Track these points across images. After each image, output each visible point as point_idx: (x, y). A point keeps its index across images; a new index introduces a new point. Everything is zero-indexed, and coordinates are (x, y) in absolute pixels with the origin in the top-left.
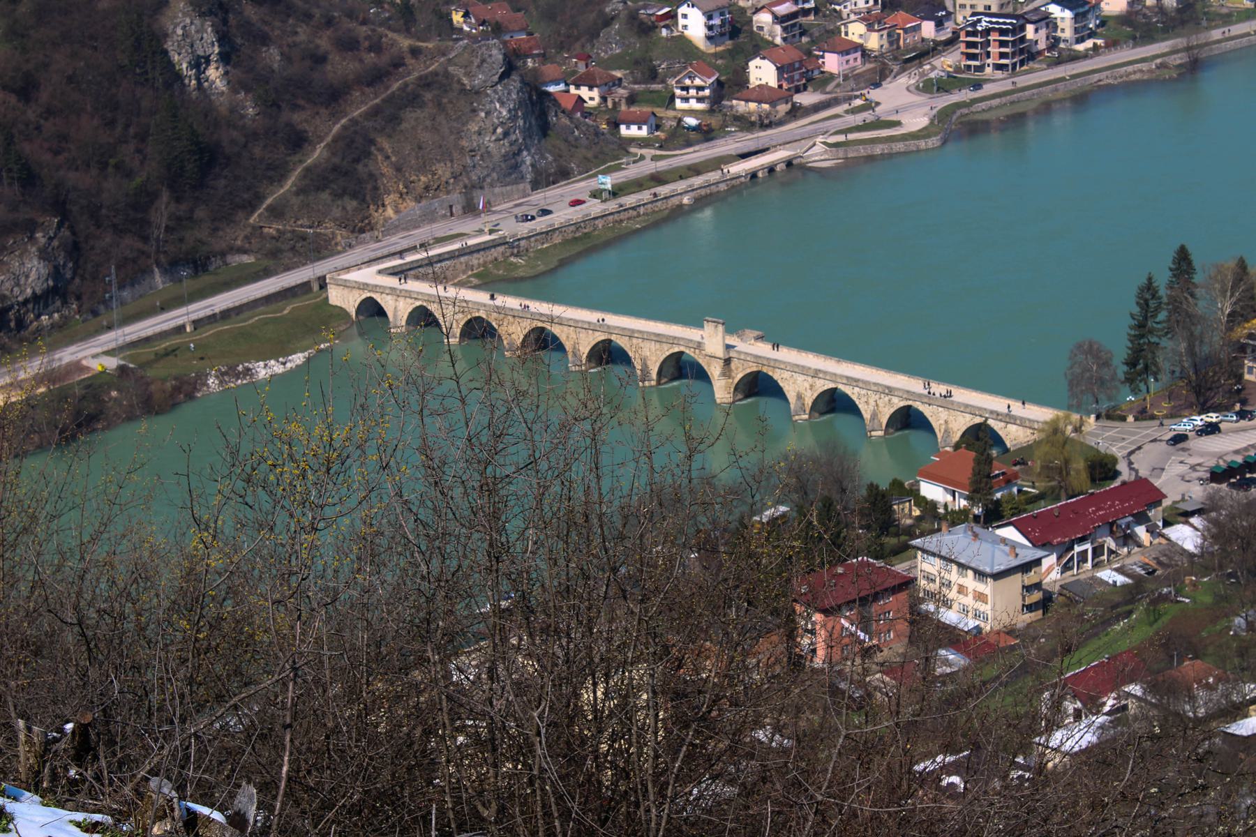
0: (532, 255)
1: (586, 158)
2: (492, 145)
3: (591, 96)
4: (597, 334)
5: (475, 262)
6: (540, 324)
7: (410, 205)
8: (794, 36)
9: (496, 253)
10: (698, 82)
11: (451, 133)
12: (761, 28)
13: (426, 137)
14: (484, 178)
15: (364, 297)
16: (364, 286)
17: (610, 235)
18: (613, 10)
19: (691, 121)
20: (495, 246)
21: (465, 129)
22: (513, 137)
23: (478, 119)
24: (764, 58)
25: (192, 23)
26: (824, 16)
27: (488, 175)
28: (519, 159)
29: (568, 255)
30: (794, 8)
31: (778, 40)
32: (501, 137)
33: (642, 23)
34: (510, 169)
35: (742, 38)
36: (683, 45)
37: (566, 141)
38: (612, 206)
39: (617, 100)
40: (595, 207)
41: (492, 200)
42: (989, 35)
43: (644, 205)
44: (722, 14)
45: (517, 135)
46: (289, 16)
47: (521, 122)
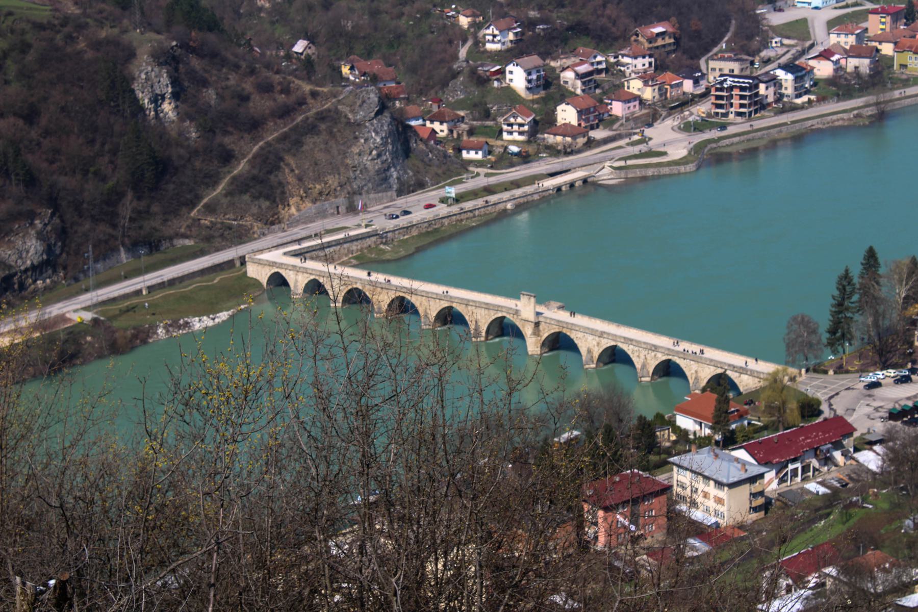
0: (396, 243)
1: (437, 174)
3: (442, 129)
4: (442, 302)
5: (354, 248)
6: (402, 294)
7: (308, 205)
8: (590, 88)
9: (370, 241)
10: (519, 120)
11: (339, 154)
12: (566, 82)
13: (321, 156)
15: (273, 271)
16: (273, 264)
17: (453, 230)
18: (459, 67)
19: (514, 149)
20: (369, 237)
21: (349, 151)
22: (384, 158)
23: (359, 144)
24: (568, 104)
25: (152, 70)
26: (613, 74)
27: (365, 185)
28: (388, 174)
29: (423, 243)
30: (591, 68)
31: (579, 91)
33: (479, 77)
34: (382, 181)
35: (552, 90)
36: (510, 94)
37: (423, 161)
38: (455, 209)
39: (460, 132)
40: (442, 210)
41: (368, 203)
42: (732, 90)
43: (478, 209)
45: (387, 156)
46: (223, 66)
47: (390, 147)
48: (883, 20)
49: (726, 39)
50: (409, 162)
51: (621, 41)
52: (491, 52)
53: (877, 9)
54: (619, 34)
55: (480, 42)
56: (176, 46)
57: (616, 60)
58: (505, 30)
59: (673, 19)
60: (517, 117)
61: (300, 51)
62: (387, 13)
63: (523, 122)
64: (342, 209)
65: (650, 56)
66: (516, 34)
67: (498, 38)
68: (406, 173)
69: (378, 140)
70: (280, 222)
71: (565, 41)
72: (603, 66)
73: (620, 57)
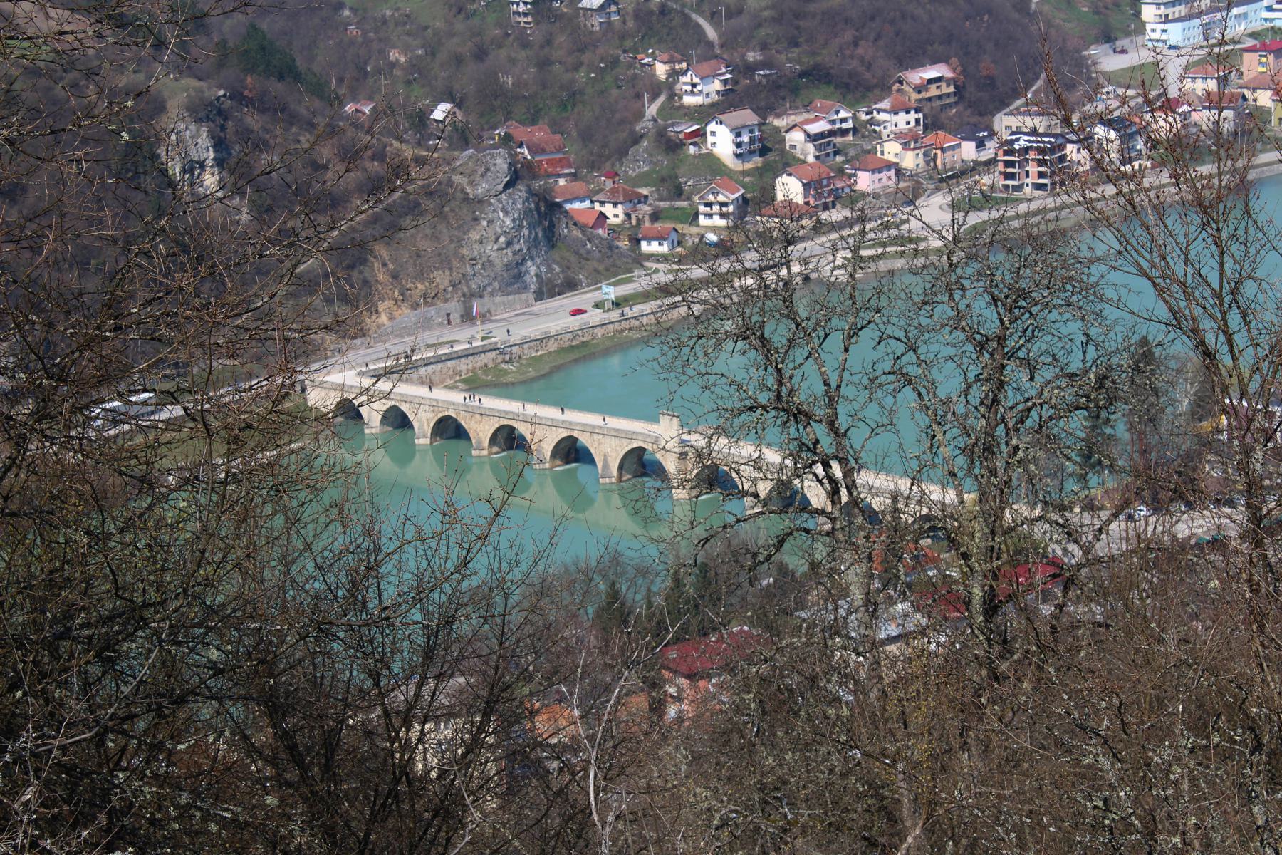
0: (524, 362)
1: (596, 271)
2: (494, 254)
3: (615, 214)
5: (463, 367)
6: (506, 422)
7: (405, 311)
8: (828, 155)
9: (488, 358)
10: (721, 198)
11: (452, 241)
12: (793, 147)
13: (428, 246)
14: (485, 288)
16: (342, 388)
17: (608, 343)
18: (643, 128)
19: (712, 237)
20: (484, 352)
21: (466, 237)
22: (517, 247)
23: (478, 228)
24: (790, 175)
25: (187, 128)
26: (863, 136)
27: (490, 284)
28: (523, 269)
29: (562, 362)
30: (828, 127)
31: (811, 159)
32: (504, 246)
33: (669, 140)
34: (513, 279)
35: (771, 157)
36: (712, 165)
37: (577, 253)
38: (614, 315)
39: (640, 217)
40: (595, 316)
41: (493, 309)
42: (1027, 154)
43: (647, 315)
44: (751, 131)
45: (521, 245)
46: (292, 124)
47: (526, 232)
48: (1264, 60)
49: (1034, 88)
50: (555, 254)
51: (877, 92)
52: (689, 107)
53: (1255, 46)
54: (875, 81)
55: (676, 95)
56: (224, 96)
57: (869, 117)
58: (708, 76)
59: (954, 60)
60: (718, 193)
61: (441, 119)
62: (560, 63)
63: (725, 200)
64: (455, 317)
65: (917, 111)
66: (725, 82)
67: (699, 88)
68: (550, 269)
69: (508, 222)
70: (364, 335)
71: (795, 91)
72: (849, 124)
73: (875, 112)
